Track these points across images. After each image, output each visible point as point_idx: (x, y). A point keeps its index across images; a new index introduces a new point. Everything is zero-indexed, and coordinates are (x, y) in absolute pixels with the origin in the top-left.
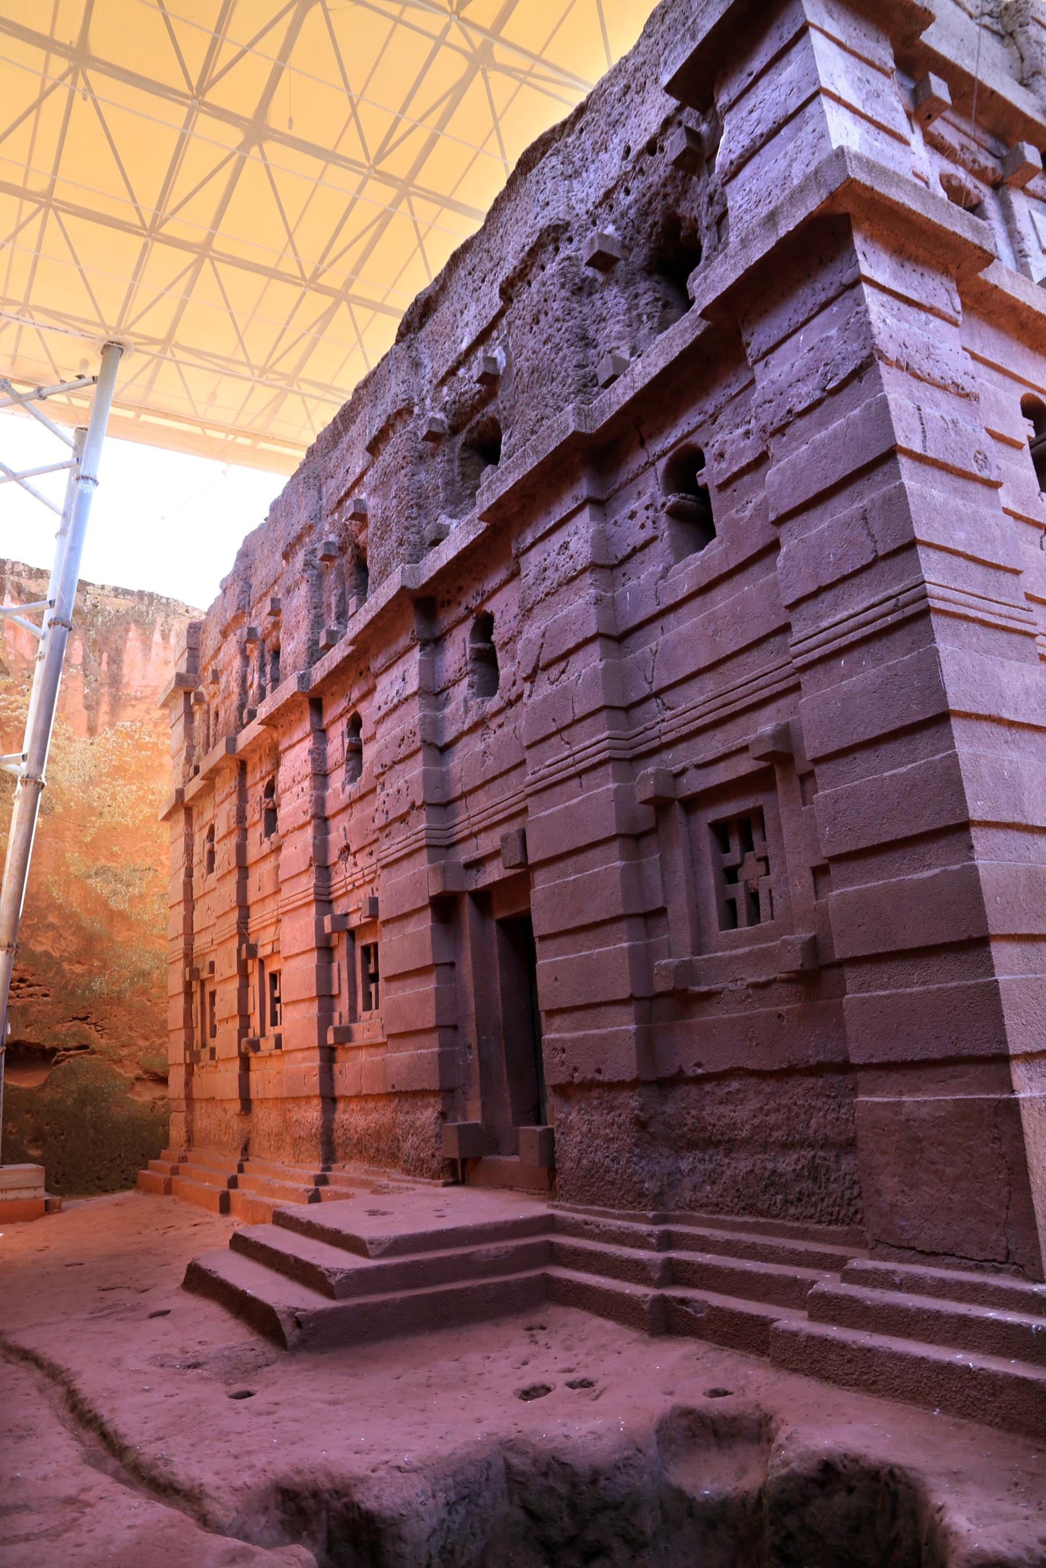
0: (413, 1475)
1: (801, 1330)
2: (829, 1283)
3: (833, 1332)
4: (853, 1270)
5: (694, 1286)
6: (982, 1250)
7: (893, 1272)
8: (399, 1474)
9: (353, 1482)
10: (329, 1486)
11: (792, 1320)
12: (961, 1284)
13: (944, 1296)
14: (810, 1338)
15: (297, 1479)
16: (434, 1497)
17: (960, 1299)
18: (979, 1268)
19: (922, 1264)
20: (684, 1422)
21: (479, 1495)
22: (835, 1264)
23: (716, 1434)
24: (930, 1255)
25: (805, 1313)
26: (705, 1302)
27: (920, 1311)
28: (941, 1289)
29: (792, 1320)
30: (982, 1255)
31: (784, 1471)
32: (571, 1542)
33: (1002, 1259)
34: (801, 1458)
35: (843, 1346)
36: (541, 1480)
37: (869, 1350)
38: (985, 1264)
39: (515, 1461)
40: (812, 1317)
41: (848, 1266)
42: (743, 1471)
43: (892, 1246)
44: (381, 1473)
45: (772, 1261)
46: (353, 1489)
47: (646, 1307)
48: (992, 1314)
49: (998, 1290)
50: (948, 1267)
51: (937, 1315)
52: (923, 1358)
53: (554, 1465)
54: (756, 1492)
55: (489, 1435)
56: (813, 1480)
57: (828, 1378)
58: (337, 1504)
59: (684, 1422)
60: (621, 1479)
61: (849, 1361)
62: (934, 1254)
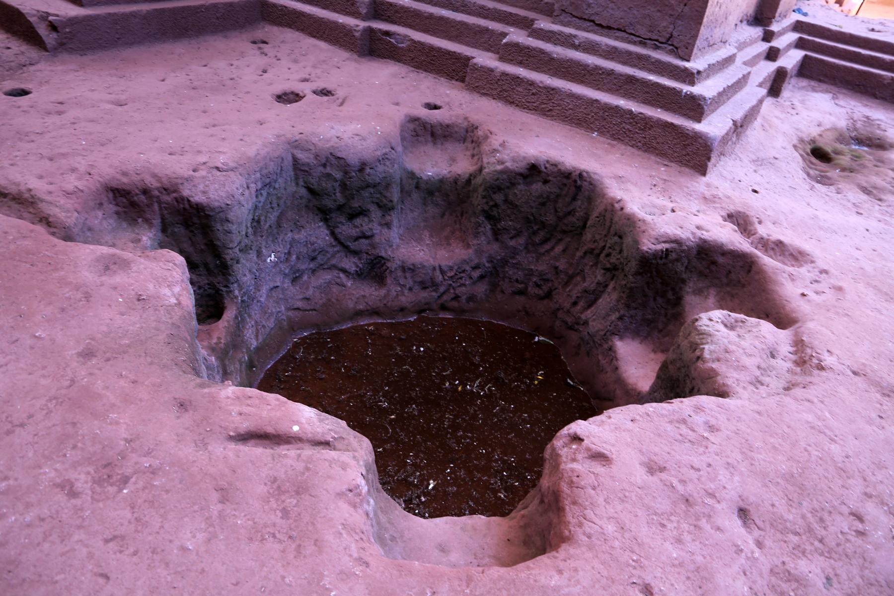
0: (231, 174)
1: (496, 68)
2: (516, 36)
3: (522, 72)
4: (541, 29)
5: (393, 22)
6: (650, 31)
7: (575, 36)
8: (219, 173)
9: (180, 181)
10: (158, 185)
11: (484, 59)
12: (629, 53)
13: (612, 59)
14: (504, 74)
15: (125, 180)
16: (248, 187)
17: (624, 63)
18: (643, 44)
19: (596, 33)
20: (411, 126)
21: (275, 181)
22: (525, 24)
23: (433, 135)
24: (605, 28)
25: (497, 56)
26: (406, 36)
27: (597, 68)
28: (612, 54)
29: (484, 59)
30: (649, 35)
31: (499, 167)
32: (340, 208)
33: (664, 40)
34: (514, 160)
35: (532, 83)
36: (321, 169)
37: (553, 89)
38: (648, 41)
39: (300, 155)
40: (502, 59)
41: (535, 26)
42: (453, 160)
43: (574, 16)
44: (202, 173)
45: (462, 12)
46: (181, 187)
47: (357, 34)
48: (652, 78)
49: (659, 62)
50: (617, 38)
51: (611, 73)
52: (597, 101)
53: (333, 160)
54: (467, 176)
55: (278, 136)
56: (521, 175)
57: (512, 103)
58: (166, 198)
59: (411, 126)
60: (381, 168)
61: (533, 94)
62: (609, 28)
